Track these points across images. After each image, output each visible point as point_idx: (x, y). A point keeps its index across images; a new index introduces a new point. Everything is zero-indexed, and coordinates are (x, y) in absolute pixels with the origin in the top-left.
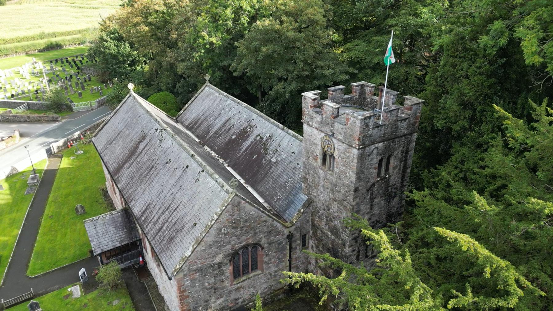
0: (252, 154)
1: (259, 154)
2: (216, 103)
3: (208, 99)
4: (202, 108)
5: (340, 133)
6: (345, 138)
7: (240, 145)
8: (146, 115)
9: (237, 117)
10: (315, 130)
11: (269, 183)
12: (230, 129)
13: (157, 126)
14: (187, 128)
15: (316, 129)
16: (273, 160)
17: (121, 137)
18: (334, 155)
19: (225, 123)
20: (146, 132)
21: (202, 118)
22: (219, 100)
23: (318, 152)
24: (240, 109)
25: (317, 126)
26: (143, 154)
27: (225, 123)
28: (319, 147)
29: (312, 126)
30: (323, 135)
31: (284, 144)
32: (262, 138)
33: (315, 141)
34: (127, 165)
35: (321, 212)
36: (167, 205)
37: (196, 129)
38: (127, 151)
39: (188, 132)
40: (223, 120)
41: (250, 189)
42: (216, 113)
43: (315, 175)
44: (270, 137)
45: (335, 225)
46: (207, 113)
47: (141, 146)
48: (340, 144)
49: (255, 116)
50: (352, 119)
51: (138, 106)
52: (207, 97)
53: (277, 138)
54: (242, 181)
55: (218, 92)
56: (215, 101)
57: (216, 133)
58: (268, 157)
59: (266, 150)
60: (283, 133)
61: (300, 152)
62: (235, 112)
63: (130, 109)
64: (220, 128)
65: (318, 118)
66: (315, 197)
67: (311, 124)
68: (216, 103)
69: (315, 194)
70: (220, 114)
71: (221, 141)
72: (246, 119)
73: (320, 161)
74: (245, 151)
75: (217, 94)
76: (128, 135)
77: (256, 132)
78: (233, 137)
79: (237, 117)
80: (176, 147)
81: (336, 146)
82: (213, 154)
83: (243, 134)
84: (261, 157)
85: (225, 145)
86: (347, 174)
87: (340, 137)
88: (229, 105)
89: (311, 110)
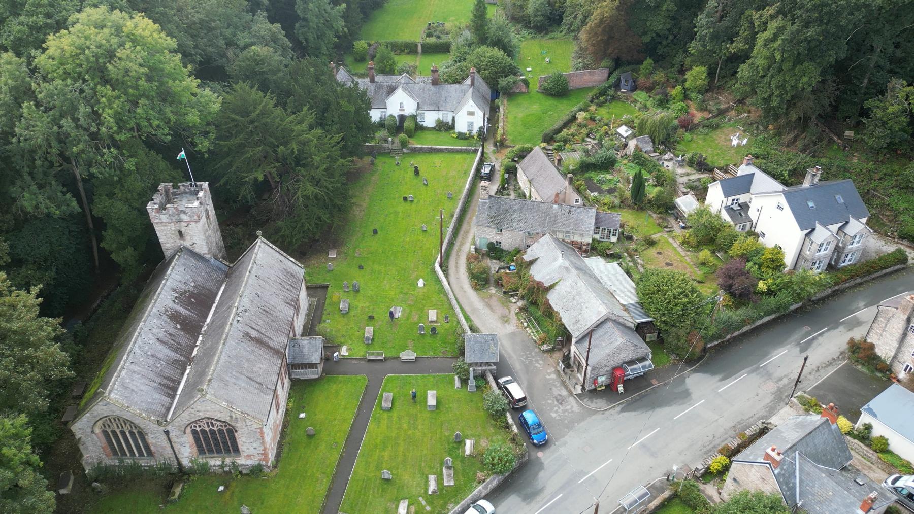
0: (191, 303)
1: (190, 297)
2: (136, 368)
3: (130, 386)
4: (143, 387)
7: (185, 317)
8: (227, 344)
9: (155, 331)
11: (210, 285)
12: (170, 334)
13: (235, 322)
14: (173, 397)
16: (193, 284)
17: (252, 371)
19: (164, 343)
20: (241, 334)
21: (158, 380)
22: (133, 367)
24: (146, 329)
26: (258, 328)
27: (164, 343)
31: (179, 277)
32: (176, 298)
34: (271, 343)
36: (280, 286)
37: (173, 381)
38: (261, 352)
39: (179, 392)
40: (160, 347)
41: (218, 298)
42: (151, 361)
44: (174, 290)
46: (152, 376)
47: (254, 334)
49: (155, 310)
51: (218, 369)
52: (126, 388)
53: (175, 285)
54: (215, 305)
55: (120, 371)
56: (134, 372)
57: (176, 350)
58: (191, 289)
59: (185, 292)
60: (170, 280)
61: (184, 265)
62: (150, 336)
63: (222, 380)
64: (170, 347)
68: (136, 368)
70: (153, 356)
71: (184, 340)
72: (159, 319)
74: (189, 310)
75: (124, 373)
76: (248, 360)
77: (171, 305)
78: (179, 326)
79: (155, 331)
80: (247, 291)
82: (200, 338)
83: (175, 317)
84: (192, 295)
85: (188, 333)
88: (140, 347)
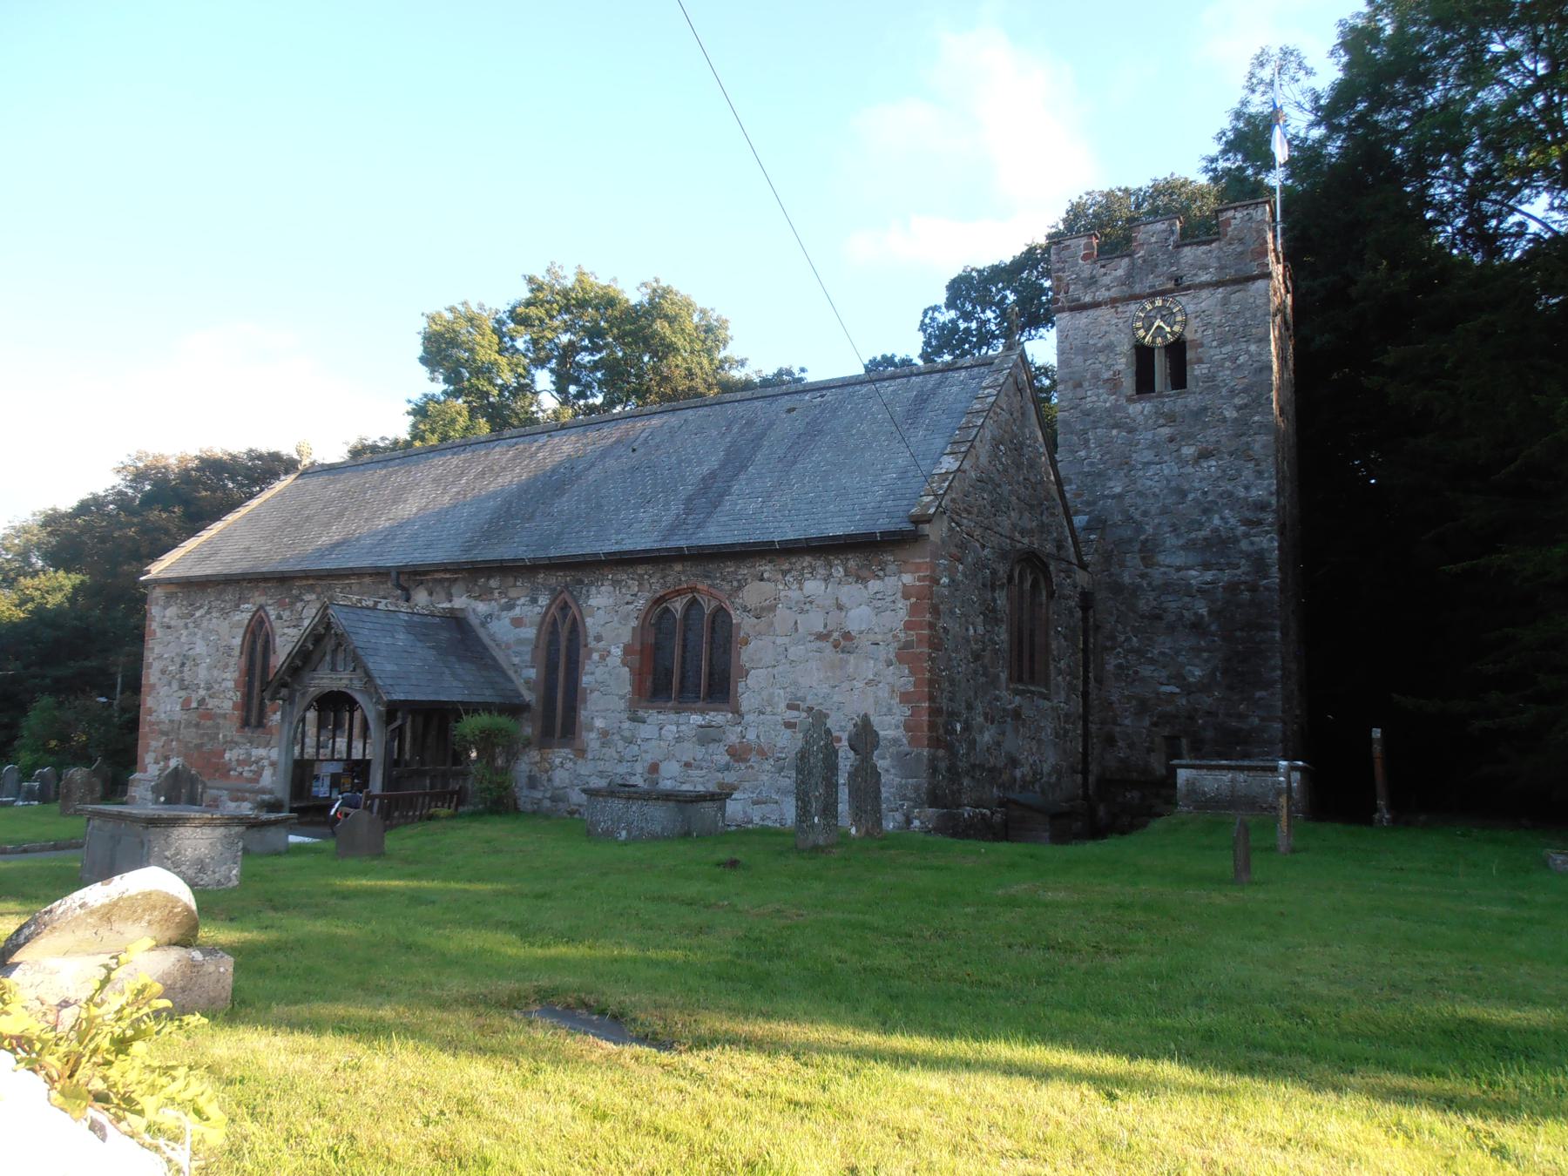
5: (1205, 268)
6: (1221, 268)
10: (1105, 313)
15: (1113, 302)
18: (1189, 336)
23: (1123, 363)
25: (1114, 293)
28: (1125, 347)
29: (1096, 305)
30: (1133, 307)
33: (1103, 341)
35: (1149, 529)
43: (1114, 432)
45: (1216, 530)
48: (1204, 293)
50: (1239, 215)
65: (1121, 267)
66: (1120, 496)
67: (1088, 299)
69: (1118, 490)
73: (1128, 383)
81: (1190, 308)
86: (1242, 359)
87: (1205, 278)
89: (1086, 269)
